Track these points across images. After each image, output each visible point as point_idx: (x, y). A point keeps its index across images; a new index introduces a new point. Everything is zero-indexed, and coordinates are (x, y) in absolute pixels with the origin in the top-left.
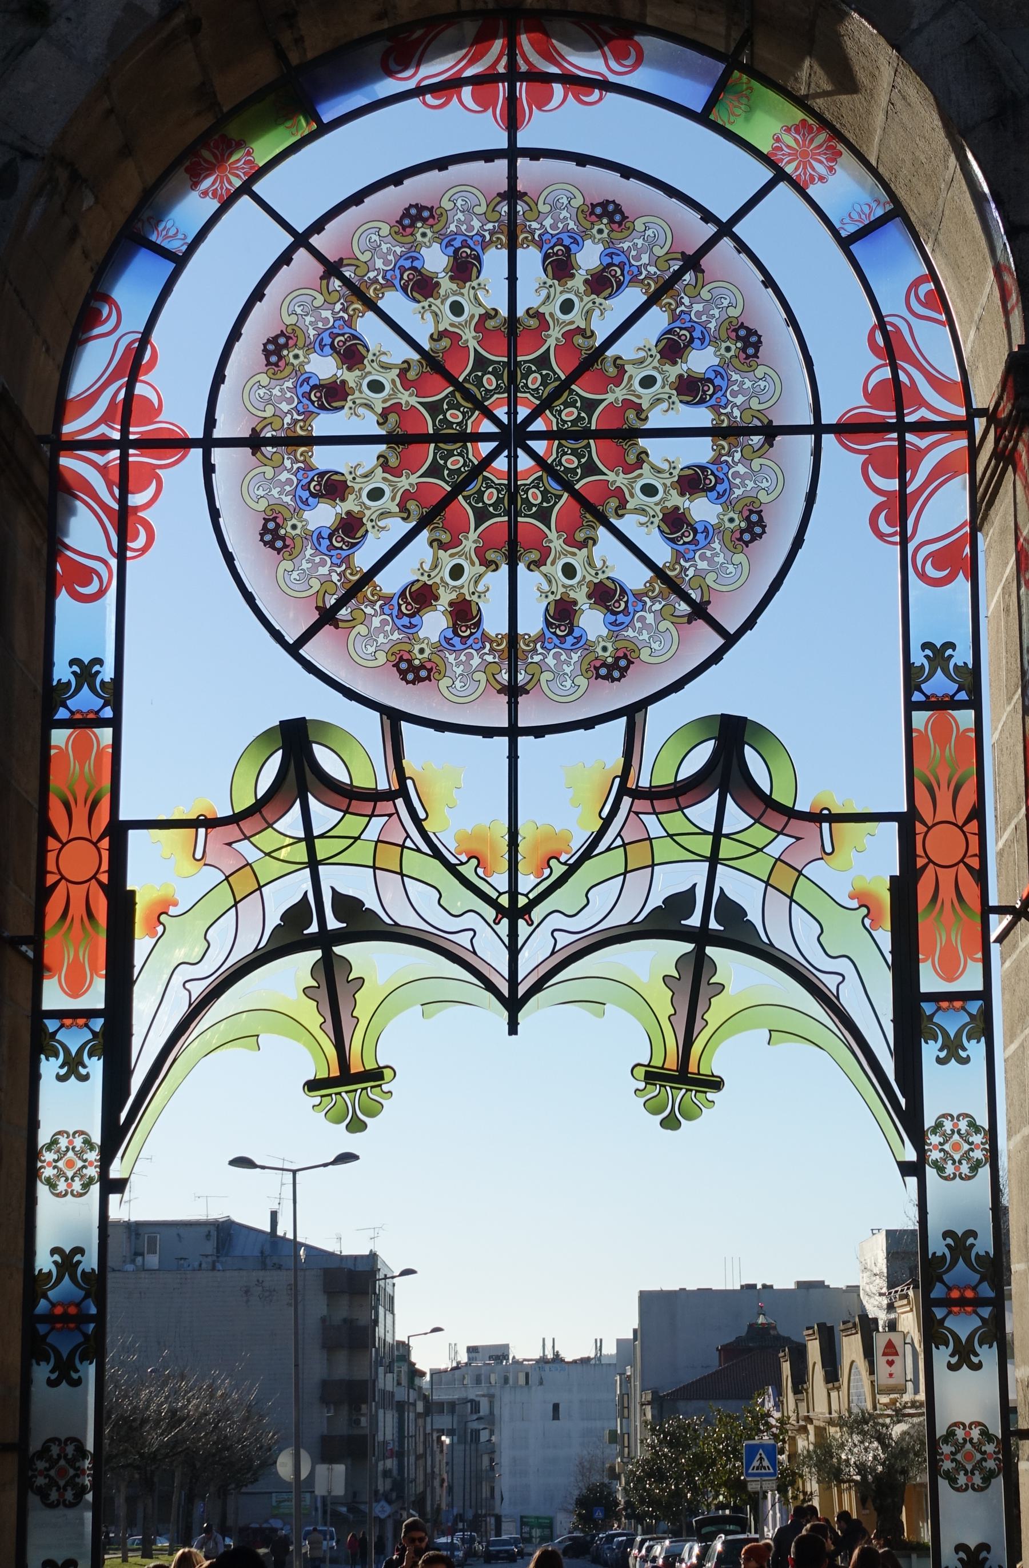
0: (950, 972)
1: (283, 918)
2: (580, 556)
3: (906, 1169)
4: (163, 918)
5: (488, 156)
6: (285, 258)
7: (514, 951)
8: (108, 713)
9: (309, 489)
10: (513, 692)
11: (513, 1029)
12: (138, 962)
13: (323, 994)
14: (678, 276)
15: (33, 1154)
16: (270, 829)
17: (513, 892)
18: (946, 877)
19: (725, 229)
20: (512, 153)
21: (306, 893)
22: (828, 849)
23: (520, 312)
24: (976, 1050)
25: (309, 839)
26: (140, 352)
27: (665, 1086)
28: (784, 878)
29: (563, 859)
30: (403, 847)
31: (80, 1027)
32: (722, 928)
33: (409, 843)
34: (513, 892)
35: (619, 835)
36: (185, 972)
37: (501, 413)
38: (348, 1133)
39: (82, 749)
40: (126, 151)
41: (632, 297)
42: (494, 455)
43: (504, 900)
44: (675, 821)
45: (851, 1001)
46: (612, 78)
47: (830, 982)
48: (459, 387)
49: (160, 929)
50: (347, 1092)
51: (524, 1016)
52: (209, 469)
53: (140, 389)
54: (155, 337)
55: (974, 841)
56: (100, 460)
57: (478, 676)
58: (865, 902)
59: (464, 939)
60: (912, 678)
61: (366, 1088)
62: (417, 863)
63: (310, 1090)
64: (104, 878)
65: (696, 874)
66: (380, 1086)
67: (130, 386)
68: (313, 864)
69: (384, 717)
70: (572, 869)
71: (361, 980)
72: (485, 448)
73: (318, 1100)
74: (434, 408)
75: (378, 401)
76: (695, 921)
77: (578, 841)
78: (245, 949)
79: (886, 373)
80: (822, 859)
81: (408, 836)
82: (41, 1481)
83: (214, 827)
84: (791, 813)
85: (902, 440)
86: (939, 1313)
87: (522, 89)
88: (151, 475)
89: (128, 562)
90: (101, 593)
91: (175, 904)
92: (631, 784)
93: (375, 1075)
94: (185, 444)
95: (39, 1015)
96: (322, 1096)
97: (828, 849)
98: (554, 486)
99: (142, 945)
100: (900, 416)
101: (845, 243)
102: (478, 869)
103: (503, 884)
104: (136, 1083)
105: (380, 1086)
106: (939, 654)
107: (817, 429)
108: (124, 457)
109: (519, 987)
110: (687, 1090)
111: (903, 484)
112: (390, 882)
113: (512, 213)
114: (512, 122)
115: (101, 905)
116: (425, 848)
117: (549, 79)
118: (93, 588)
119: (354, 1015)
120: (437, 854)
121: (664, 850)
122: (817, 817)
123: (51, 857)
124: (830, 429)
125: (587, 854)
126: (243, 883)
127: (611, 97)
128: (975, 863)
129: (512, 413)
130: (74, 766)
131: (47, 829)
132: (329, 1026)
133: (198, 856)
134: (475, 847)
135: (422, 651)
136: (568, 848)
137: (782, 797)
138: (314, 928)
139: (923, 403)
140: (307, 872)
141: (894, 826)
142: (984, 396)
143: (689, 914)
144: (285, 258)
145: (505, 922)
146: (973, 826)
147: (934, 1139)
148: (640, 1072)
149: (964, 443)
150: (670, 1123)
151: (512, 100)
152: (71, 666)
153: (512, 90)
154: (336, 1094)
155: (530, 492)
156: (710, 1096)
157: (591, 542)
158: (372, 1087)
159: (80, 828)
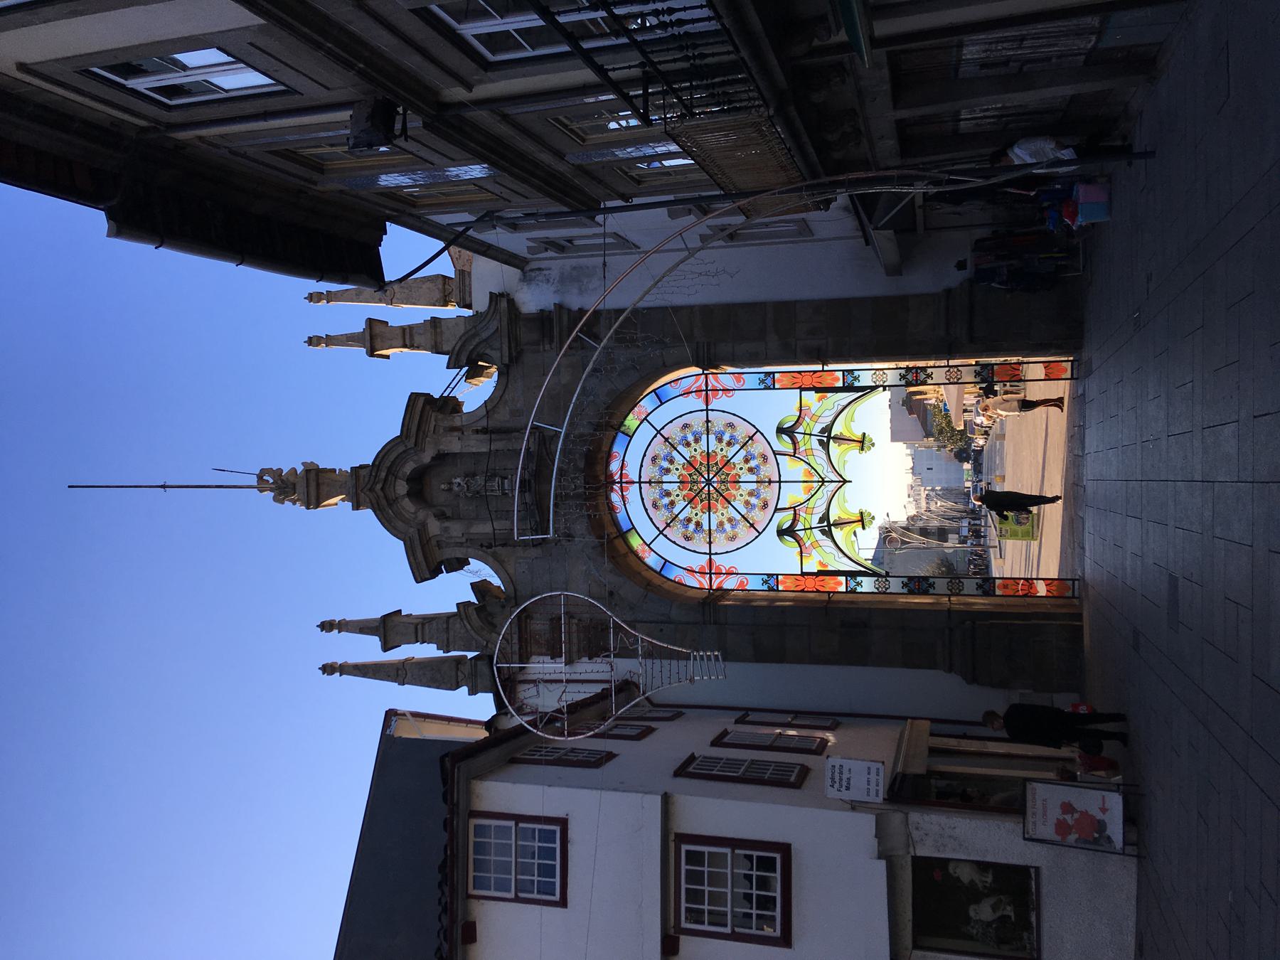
0: (837, 379)
2: (737, 466)
3: (884, 390)
5: (640, 488)
6: (666, 536)
7: (832, 481)
8: (775, 577)
10: (770, 482)
11: (850, 482)
12: (834, 569)
14: (670, 443)
15: (880, 593)
17: (819, 482)
18: (815, 380)
19: (659, 432)
20: (640, 482)
23: (679, 480)
24: (856, 373)
25: (805, 529)
26: (688, 570)
28: (816, 418)
34: (819, 482)
36: (837, 558)
37: (703, 485)
39: (783, 583)
40: (640, 573)
41: (675, 453)
42: (713, 487)
43: (820, 484)
44: (801, 444)
45: (845, 402)
46: (622, 458)
47: (840, 408)
48: (697, 495)
51: (847, 480)
53: (697, 570)
55: (806, 373)
58: (820, 399)
59: (829, 493)
60: (767, 388)
64: (814, 577)
67: (696, 572)
68: (811, 528)
70: (812, 468)
71: (839, 517)
72: (711, 488)
74: (702, 501)
75: (700, 514)
76: (825, 439)
77: (807, 467)
79: (693, 394)
82: (957, 591)
84: (800, 416)
85: (710, 390)
86: (919, 382)
87: (624, 480)
90: (746, 579)
92: (793, 454)
94: (710, 559)
95: (847, 592)
99: (830, 568)
100: (704, 390)
101: (662, 404)
103: (815, 485)
104: (863, 569)
106: (762, 381)
107: (707, 410)
108: (713, 574)
111: (721, 390)
113: (654, 482)
114: (633, 482)
115: (821, 578)
117: (621, 474)
120: (809, 500)
121: (808, 446)
122: (801, 410)
123: (809, 590)
124: (707, 407)
125: (809, 464)
127: (625, 459)
128: (812, 373)
129: (703, 482)
131: (802, 591)
134: (807, 490)
137: (796, 419)
138: (826, 528)
139: (701, 385)
141: (803, 392)
142: (700, 371)
144: (666, 536)
146: (802, 374)
147: (878, 383)
148: (861, 452)
149: (710, 375)
150: (873, 445)
151: (627, 483)
153: (624, 483)
156: (867, 435)
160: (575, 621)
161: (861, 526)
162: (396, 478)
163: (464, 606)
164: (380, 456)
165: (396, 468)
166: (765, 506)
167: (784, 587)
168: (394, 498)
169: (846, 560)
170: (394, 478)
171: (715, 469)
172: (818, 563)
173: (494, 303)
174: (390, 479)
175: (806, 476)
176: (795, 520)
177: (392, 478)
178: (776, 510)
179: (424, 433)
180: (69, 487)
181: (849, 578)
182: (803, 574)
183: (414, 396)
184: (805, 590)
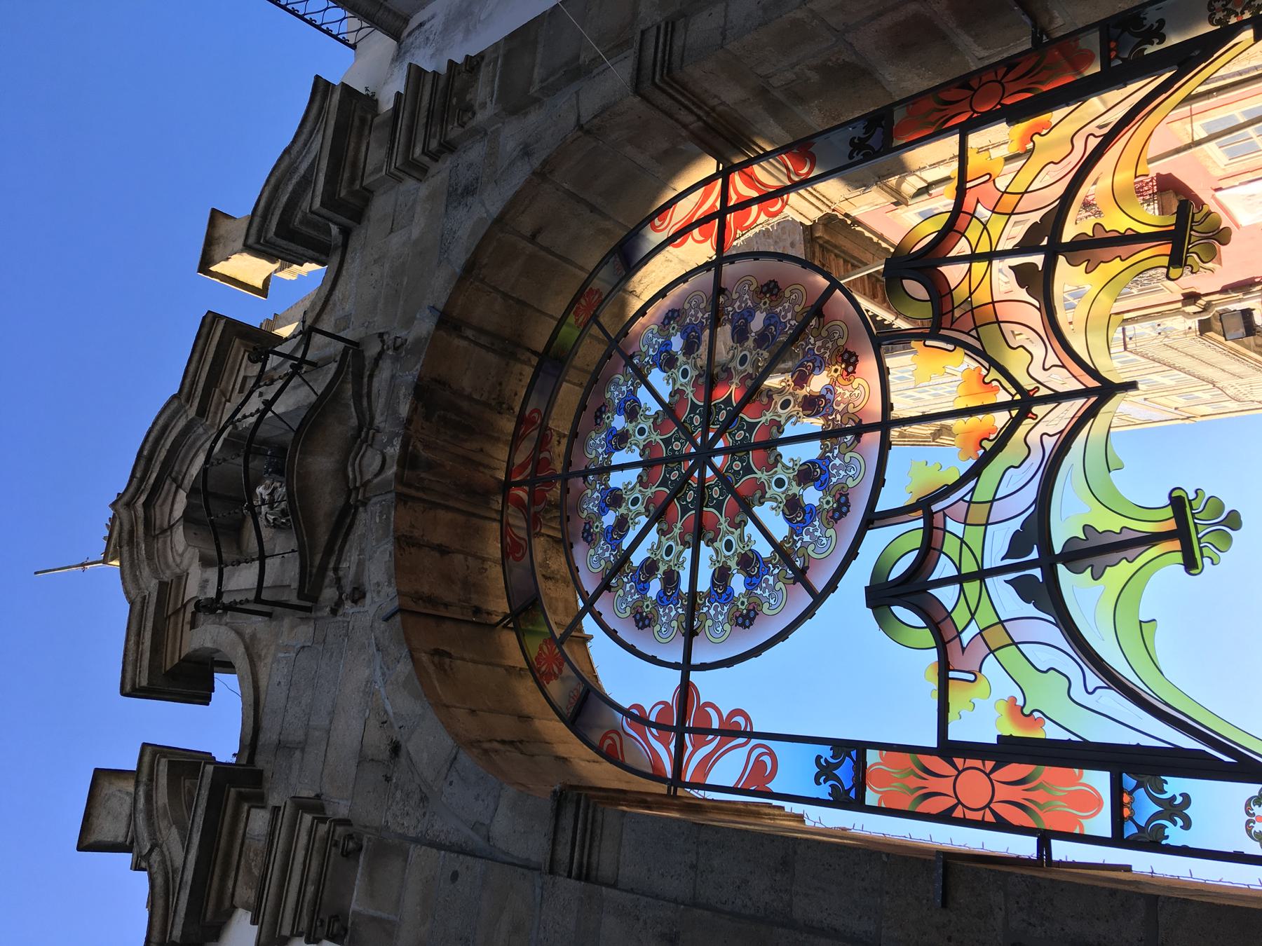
1: (1029, 602)
4: (1027, 711)
7: (1057, 398)
9: (721, 593)
11: (1132, 386)
12: (1065, 736)
13: (1098, 560)
16: (952, 615)
21: (1006, 581)
22: (988, 177)
27: (1188, 249)
29: (984, 372)
30: (970, 502)
31: (1132, 800)
32: (1046, 238)
33: (967, 498)
35: (968, 334)
38: (1243, 528)
39: (885, 779)
49: (1036, 715)
50: (1197, 533)
51: (1116, 379)
52: (704, 667)
54: (626, 706)
56: (690, 749)
57: (847, 459)
59: (1050, 443)
61: (1193, 514)
62: (985, 487)
63: (1196, 566)
64: (990, 765)
65: (1002, 268)
66: (1190, 501)
69: (871, 526)
71: (1086, 528)
73: (1207, 561)
78: (1055, 635)
80: (994, 180)
81: (962, 499)
83: (948, 663)
88: (702, 708)
89: (755, 730)
90: (772, 754)
91: (1015, 699)
93: (1178, 503)
96: (1202, 556)
97: (988, 177)
98: (736, 423)
99: (1051, 732)
102: (991, 438)
105: (1190, 501)
108: (690, 730)
109: (1090, 386)
110: (1192, 229)
112: (999, 510)
116: (972, 484)
118: (767, 759)
119: (1118, 531)
126: (996, 637)
130: (895, 787)
132: (1131, 553)
133: (971, 677)
135: (828, 502)
136: (977, 370)
138: (1037, 572)
140: (988, 581)
143: (1034, 265)
145: (1035, 410)
152: (820, 784)
154: (1199, 543)
155: (737, 439)
157: (770, 393)
158: (1192, 508)
159: (945, 785)
160: (308, 818)
161: (1179, 557)
162: (179, 487)
163: (154, 755)
164: (151, 439)
165: (181, 466)
166: (841, 508)
167: (884, 796)
168: (166, 525)
169: (1112, 701)
170: (174, 486)
171: (740, 435)
172: (1002, 708)
173: (318, 98)
174: (166, 487)
175: (971, 394)
176: (929, 551)
177: (171, 484)
178: (872, 519)
179: (223, 393)
180: (36, 573)
181: (1129, 782)
182: (948, 749)
183: (208, 320)
184: (958, 813)
